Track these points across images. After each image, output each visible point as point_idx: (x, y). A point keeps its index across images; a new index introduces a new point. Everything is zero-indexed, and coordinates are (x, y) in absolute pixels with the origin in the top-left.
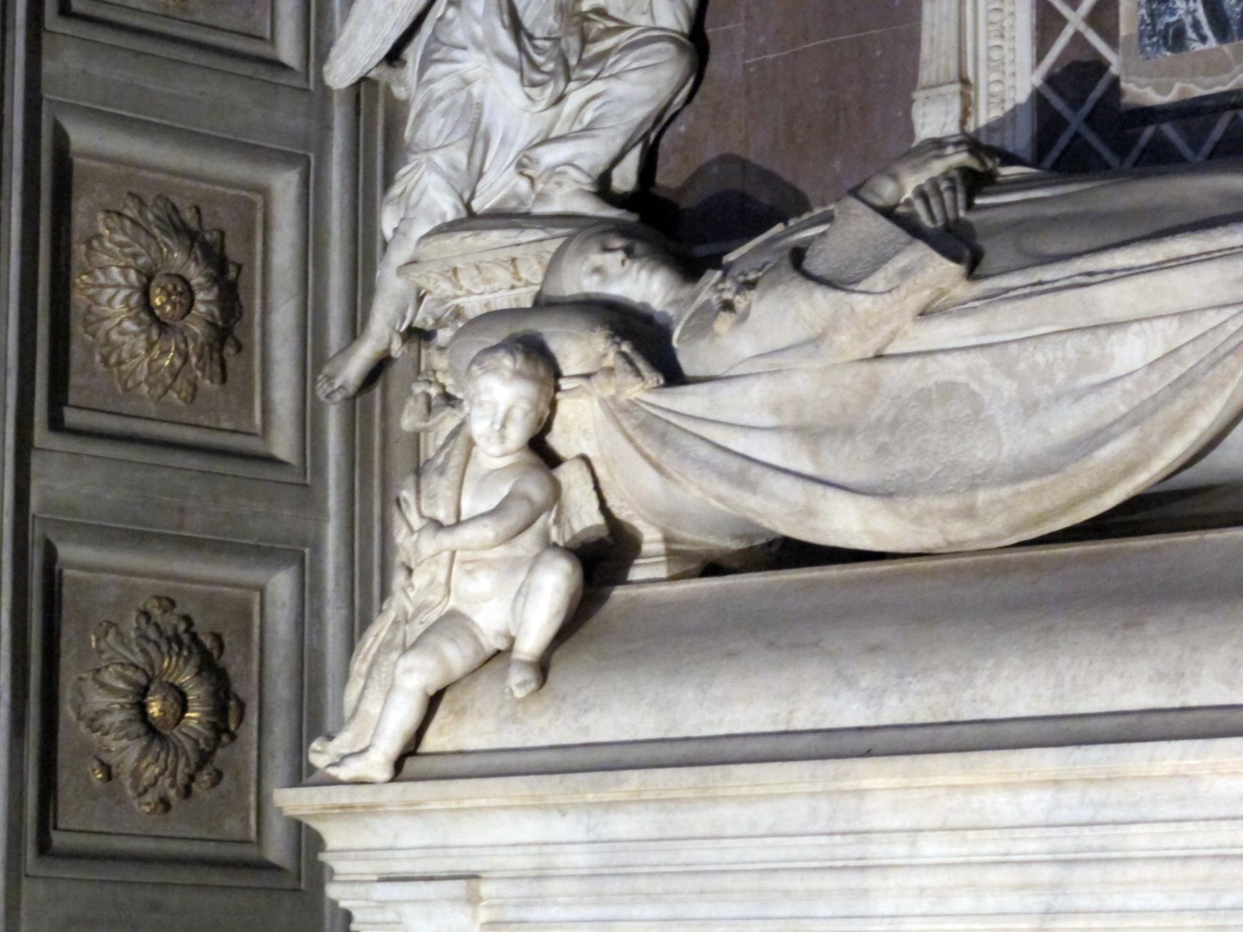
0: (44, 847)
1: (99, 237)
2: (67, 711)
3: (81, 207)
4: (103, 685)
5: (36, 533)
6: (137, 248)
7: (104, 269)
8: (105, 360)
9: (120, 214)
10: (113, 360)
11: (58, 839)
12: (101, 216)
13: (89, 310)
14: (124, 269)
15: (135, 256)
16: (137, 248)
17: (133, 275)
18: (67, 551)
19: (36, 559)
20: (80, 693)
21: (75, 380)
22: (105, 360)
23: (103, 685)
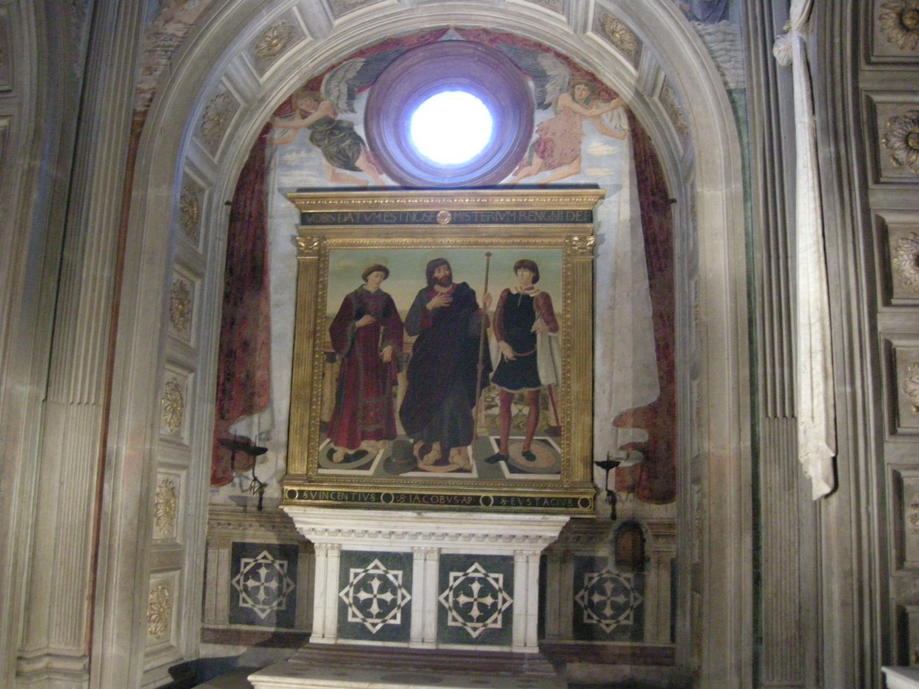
0: (893, 432)
1: (900, 247)
2: (901, 391)
3: (893, 241)
4: (913, 382)
5: (881, 338)
6: (912, 248)
7: (902, 256)
8: (906, 283)
9: (907, 239)
10: (909, 282)
11: (900, 430)
12: (900, 241)
13: (899, 269)
14: (908, 256)
15: (912, 250)
16: (912, 248)
17: (911, 256)
18: (896, 342)
19: (882, 346)
20: (905, 384)
21: (896, 290)
22: (906, 283)
23: (913, 382)
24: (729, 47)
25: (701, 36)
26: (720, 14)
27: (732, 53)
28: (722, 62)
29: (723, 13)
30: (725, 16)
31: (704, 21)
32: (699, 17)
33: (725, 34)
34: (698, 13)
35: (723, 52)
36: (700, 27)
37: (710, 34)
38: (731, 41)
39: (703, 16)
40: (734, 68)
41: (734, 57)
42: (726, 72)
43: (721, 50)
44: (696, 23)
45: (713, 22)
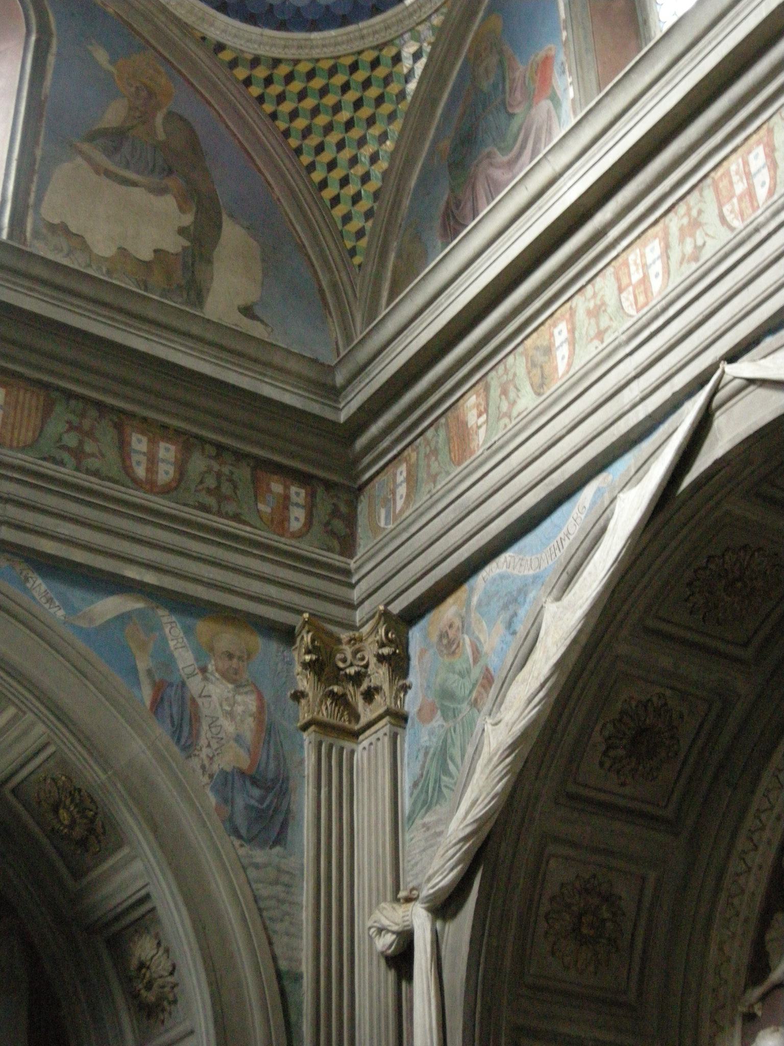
24: (282, 895)
25: (244, 868)
26: (273, 835)
27: (286, 907)
28: (271, 919)
29: (279, 834)
30: (280, 840)
31: (250, 840)
32: (243, 832)
33: (279, 870)
34: (241, 821)
35: (273, 903)
36: (241, 852)
37: (257, 866)
38: (288, 886)
39: (248, 830)
40: (288, 934)
41: (288, 914)
42: (275, 939)
43: (270, 897)
44: (237, 843)
45: (262, 846)
